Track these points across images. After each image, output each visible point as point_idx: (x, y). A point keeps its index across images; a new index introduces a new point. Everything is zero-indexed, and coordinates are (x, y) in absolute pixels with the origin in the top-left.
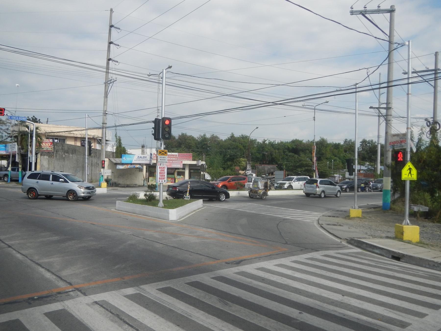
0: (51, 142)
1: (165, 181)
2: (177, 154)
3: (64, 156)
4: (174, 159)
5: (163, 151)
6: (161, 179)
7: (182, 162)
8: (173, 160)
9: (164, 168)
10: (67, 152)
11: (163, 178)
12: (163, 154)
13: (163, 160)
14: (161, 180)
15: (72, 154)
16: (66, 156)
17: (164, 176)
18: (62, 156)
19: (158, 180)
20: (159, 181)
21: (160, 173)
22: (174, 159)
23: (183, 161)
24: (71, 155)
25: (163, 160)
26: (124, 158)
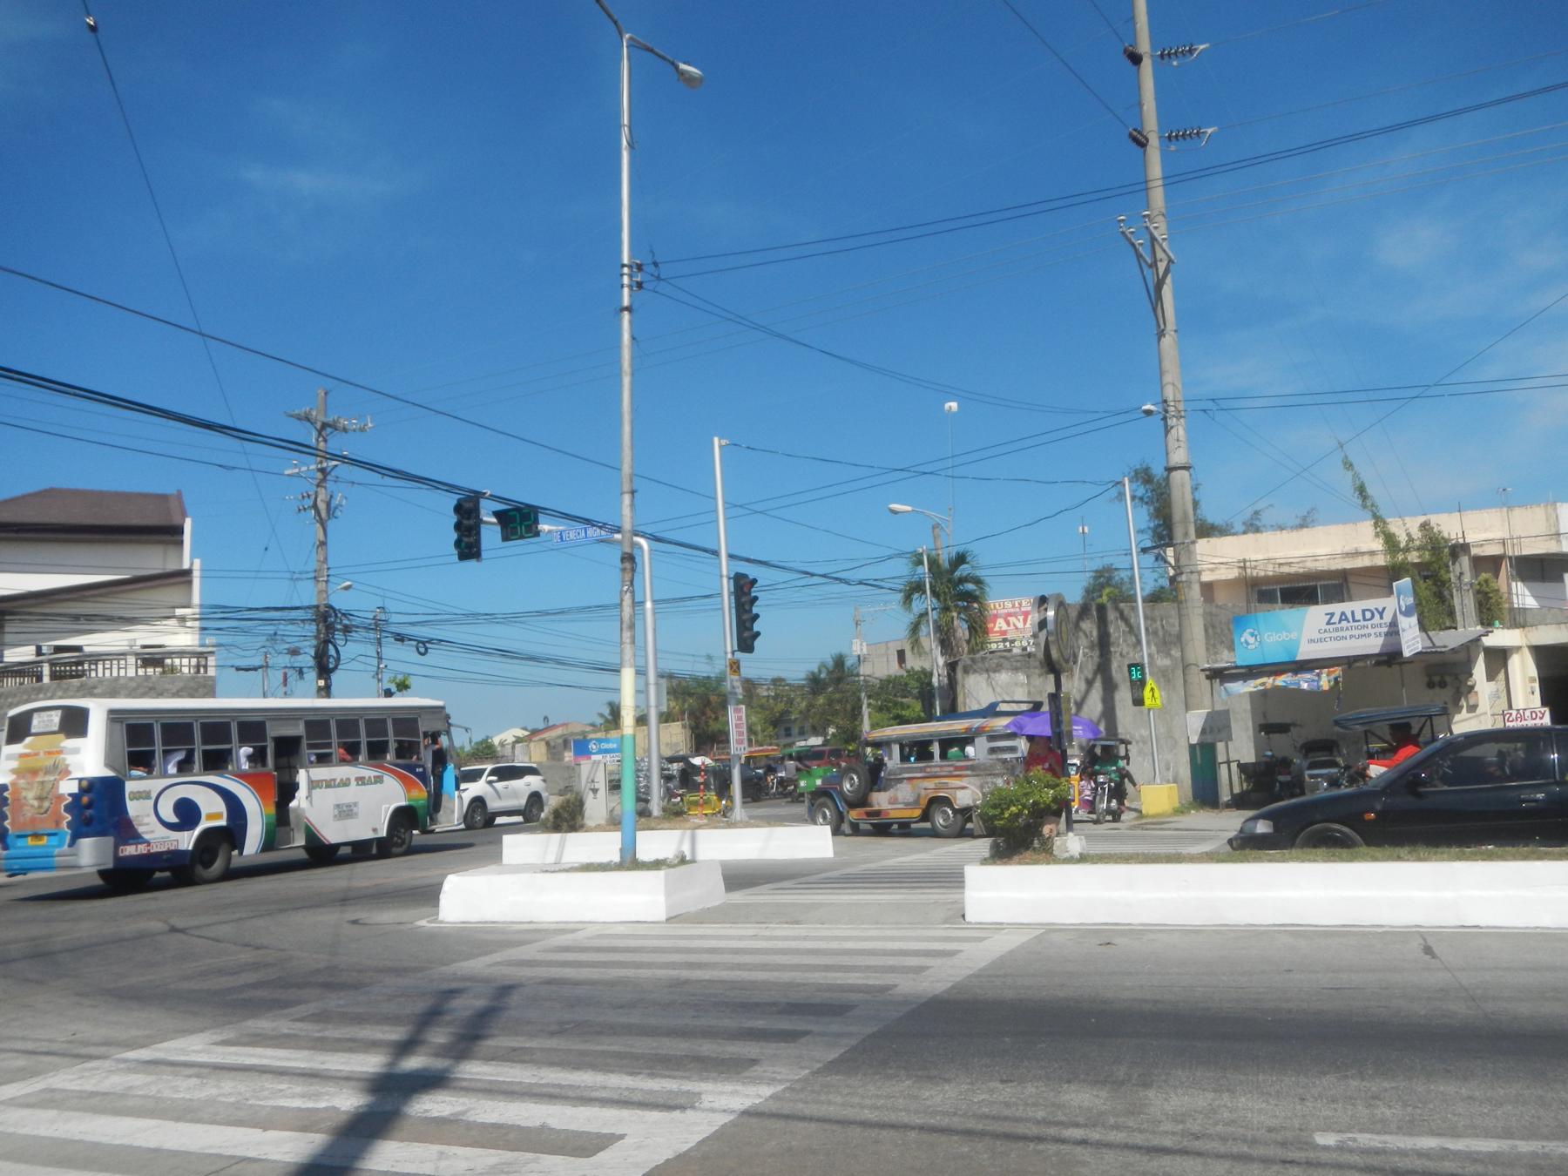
26: (1246, 636)
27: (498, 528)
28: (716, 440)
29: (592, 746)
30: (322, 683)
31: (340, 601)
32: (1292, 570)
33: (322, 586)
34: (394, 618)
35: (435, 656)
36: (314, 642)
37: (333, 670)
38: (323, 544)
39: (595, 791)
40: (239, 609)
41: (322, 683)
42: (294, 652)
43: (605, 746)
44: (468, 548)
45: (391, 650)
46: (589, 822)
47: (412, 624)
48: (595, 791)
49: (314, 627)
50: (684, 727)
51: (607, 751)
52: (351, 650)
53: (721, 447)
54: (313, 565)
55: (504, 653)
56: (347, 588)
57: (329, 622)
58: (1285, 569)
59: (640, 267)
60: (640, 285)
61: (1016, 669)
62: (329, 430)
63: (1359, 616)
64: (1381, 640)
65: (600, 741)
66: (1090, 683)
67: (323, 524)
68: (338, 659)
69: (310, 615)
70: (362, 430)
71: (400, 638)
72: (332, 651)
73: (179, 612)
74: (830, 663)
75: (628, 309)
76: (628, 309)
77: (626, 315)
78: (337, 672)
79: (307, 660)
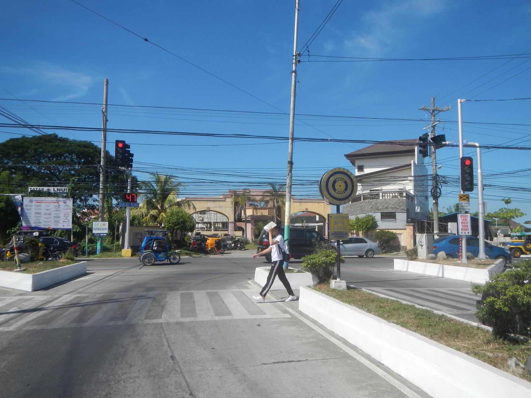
28: (459, 100)
31: (440, 172)
37: (440, 196)
39: (422, 246)
41: (434, 201)
46: (420, 257)
48: (422, 246)
53: (461, 102)
55: (524, 189)
59: (299, 55)
60: (299, 61)
62: (436, 112)
68: (441, 193)
70: (449, 109)
72: (438, 190)
73: (409, 178)
76: (293, 72)
77: (293, 74)
78: (441, 197)
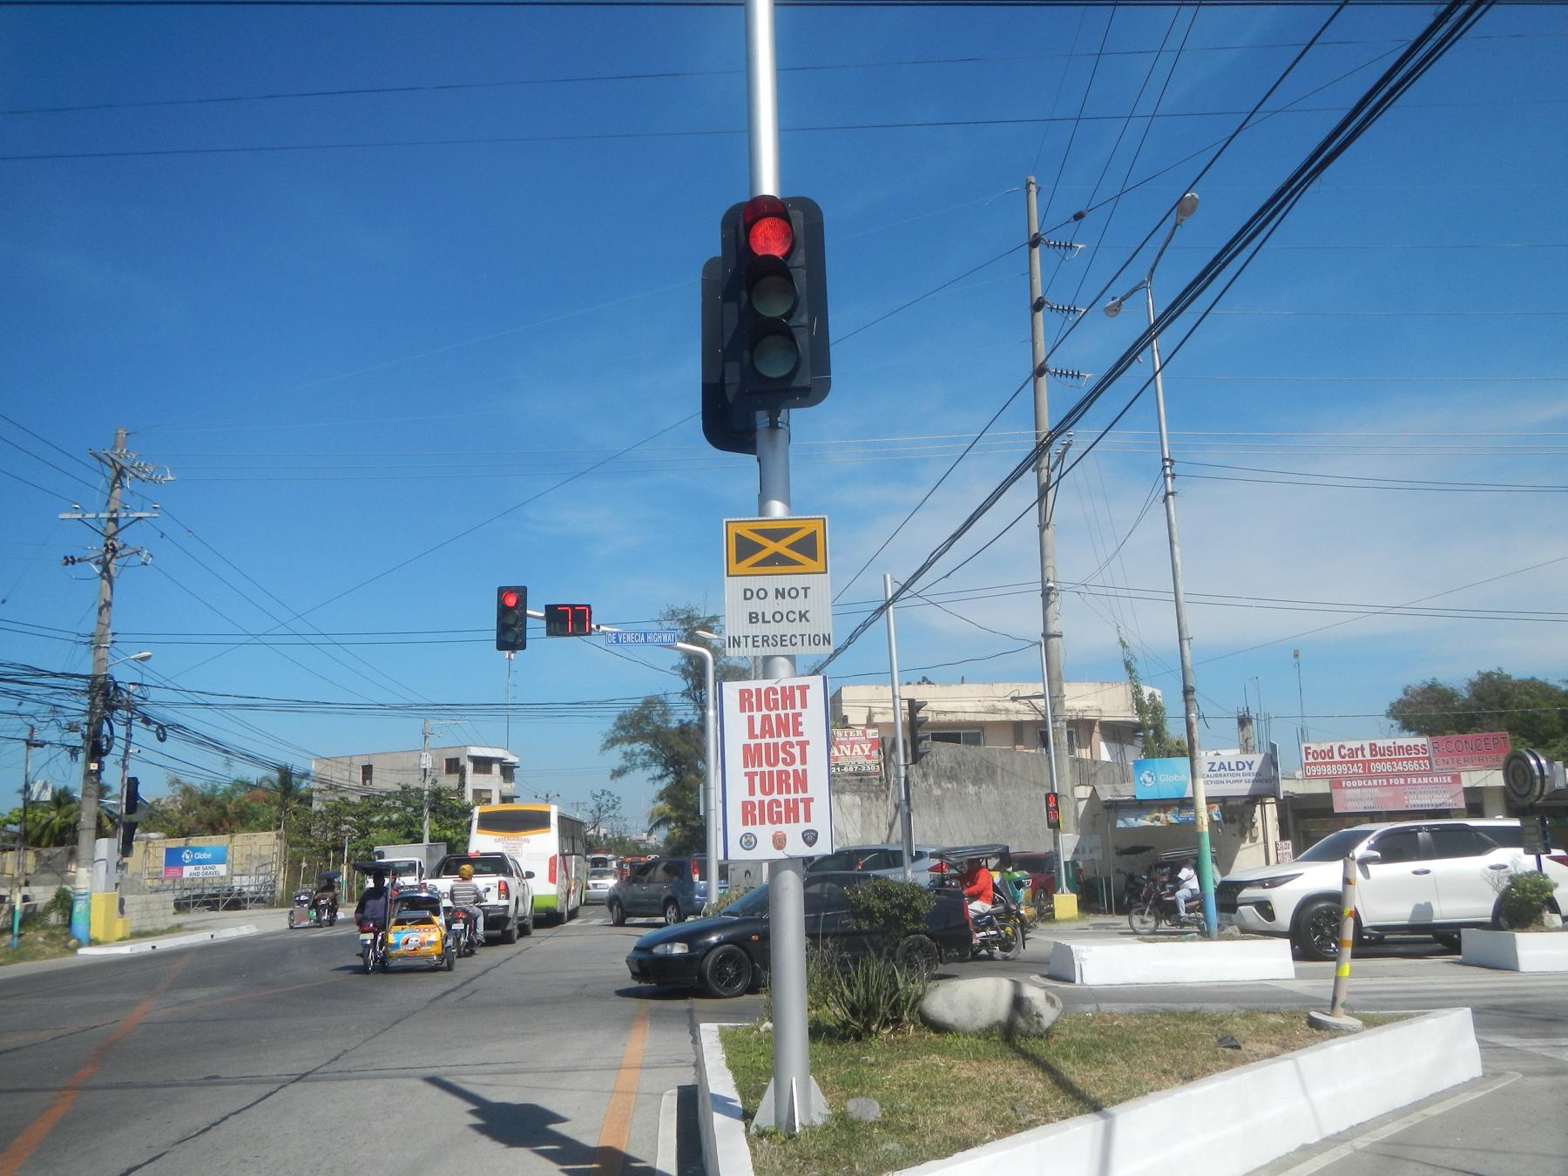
0: (872, 741)
1: (810, 838)
2: (1422, 741)
3: (937, 792)
4: (1414, 766)
5: (776, 535)
6: (769, 814)
7: (1456, 779)
8: (1410, 774)
9: (788, 696)
10: (952, 777)
11: (791, 813)
12: (776, 560)
13: (779, 617)
14: (764, 832)
15: (977, 781)
16: (945, 791)
17: (801, 781)
18: (929, 792)
19: (737, 829)
20: (749, 842)
21: (751, 755)
22: (1414, 766)
23: (1464, 776)
24: (971, 789)
25: (779, 617)
26: (1144, 776)
27: (544, 623)
29: (186, 856)
30: (94, 766)
31: (123, 675)
32: (949, 717)
33: (101, 653)
34: (154, 695)
35: (173, 745)
36: (86, 719)
37: (107, 752)
38: (108, 604)
40: (41, 673)
42: (72, 728)
43: (200, 856)
44: (510, 634)
45: (138, 729)
47: (161, 704)
49: (86, 700)
50: (279, 837)
51: (200, 862)
52: (120, 731)
54: (90, 627)
56: (143, 659)
57: (106, 696)
58: (942, 718)
61: (854, 792)
63: (1233, 766)
64: (1249, 786)
65: (195, 850)
66: (897, 807)
67: (110, 580)
68: (110, 740)
69: (82, 685)
71: (147, 721)
74: (275, 776)
75: (1173, 494)
79: (76, 739)
